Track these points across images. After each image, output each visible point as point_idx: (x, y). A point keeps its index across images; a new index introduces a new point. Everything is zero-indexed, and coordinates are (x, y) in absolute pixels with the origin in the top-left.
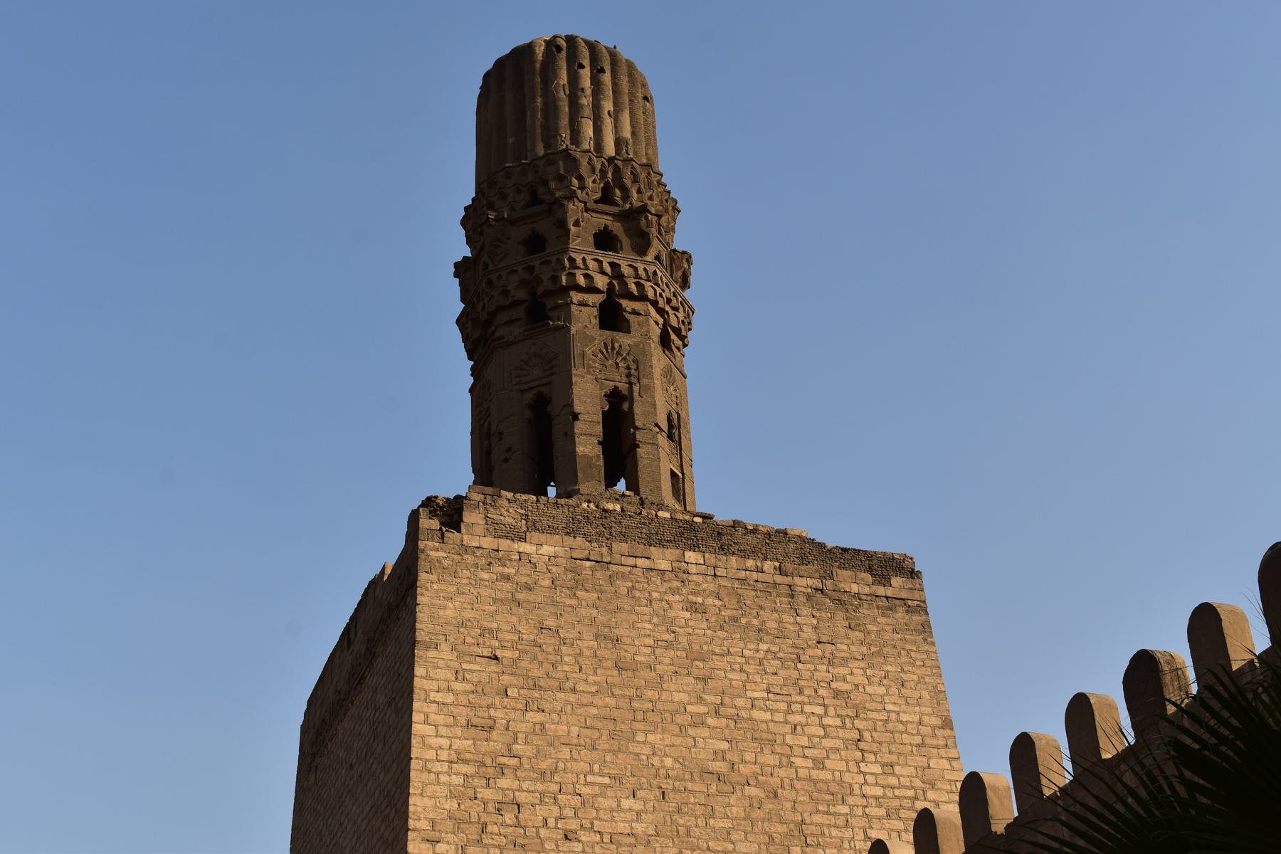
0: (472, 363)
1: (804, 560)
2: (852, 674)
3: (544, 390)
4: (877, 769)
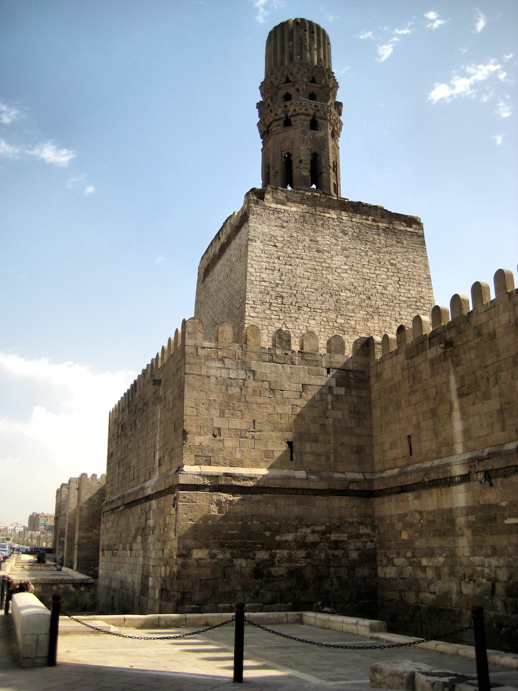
0: (262, 140)
1: (382, 217)
2: (397, 258)
3: (290, 151)
4: (404, 291)
